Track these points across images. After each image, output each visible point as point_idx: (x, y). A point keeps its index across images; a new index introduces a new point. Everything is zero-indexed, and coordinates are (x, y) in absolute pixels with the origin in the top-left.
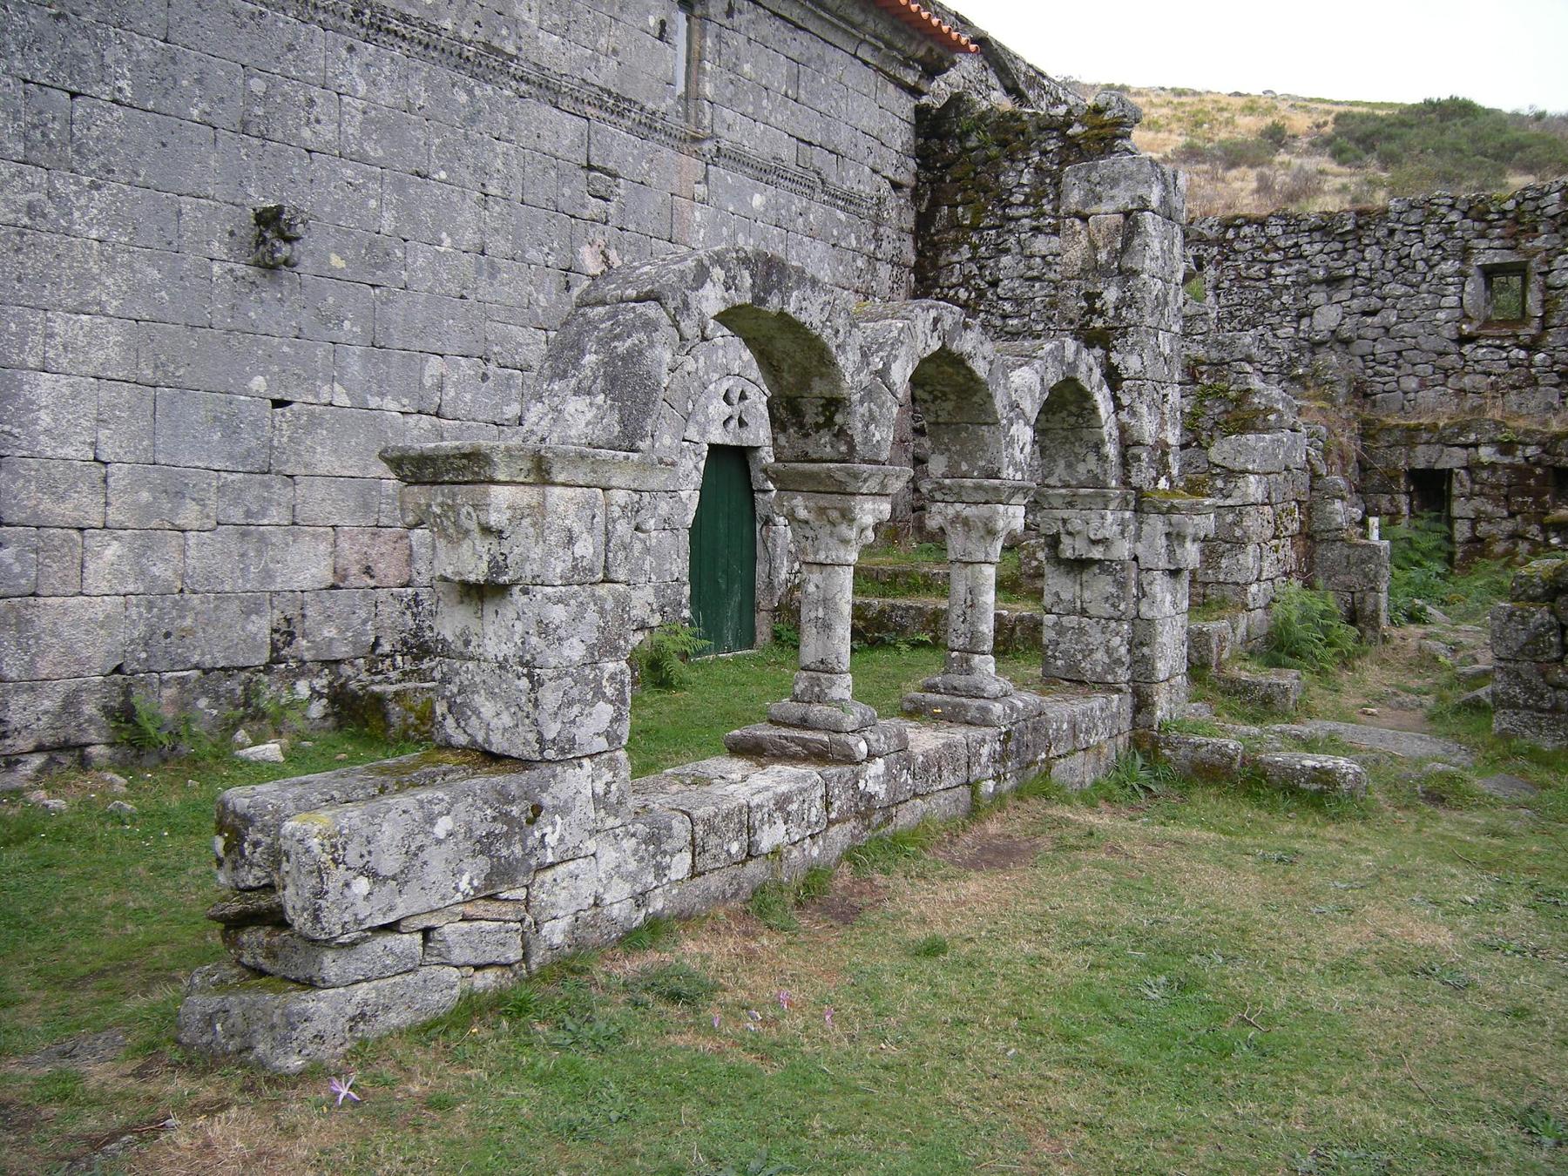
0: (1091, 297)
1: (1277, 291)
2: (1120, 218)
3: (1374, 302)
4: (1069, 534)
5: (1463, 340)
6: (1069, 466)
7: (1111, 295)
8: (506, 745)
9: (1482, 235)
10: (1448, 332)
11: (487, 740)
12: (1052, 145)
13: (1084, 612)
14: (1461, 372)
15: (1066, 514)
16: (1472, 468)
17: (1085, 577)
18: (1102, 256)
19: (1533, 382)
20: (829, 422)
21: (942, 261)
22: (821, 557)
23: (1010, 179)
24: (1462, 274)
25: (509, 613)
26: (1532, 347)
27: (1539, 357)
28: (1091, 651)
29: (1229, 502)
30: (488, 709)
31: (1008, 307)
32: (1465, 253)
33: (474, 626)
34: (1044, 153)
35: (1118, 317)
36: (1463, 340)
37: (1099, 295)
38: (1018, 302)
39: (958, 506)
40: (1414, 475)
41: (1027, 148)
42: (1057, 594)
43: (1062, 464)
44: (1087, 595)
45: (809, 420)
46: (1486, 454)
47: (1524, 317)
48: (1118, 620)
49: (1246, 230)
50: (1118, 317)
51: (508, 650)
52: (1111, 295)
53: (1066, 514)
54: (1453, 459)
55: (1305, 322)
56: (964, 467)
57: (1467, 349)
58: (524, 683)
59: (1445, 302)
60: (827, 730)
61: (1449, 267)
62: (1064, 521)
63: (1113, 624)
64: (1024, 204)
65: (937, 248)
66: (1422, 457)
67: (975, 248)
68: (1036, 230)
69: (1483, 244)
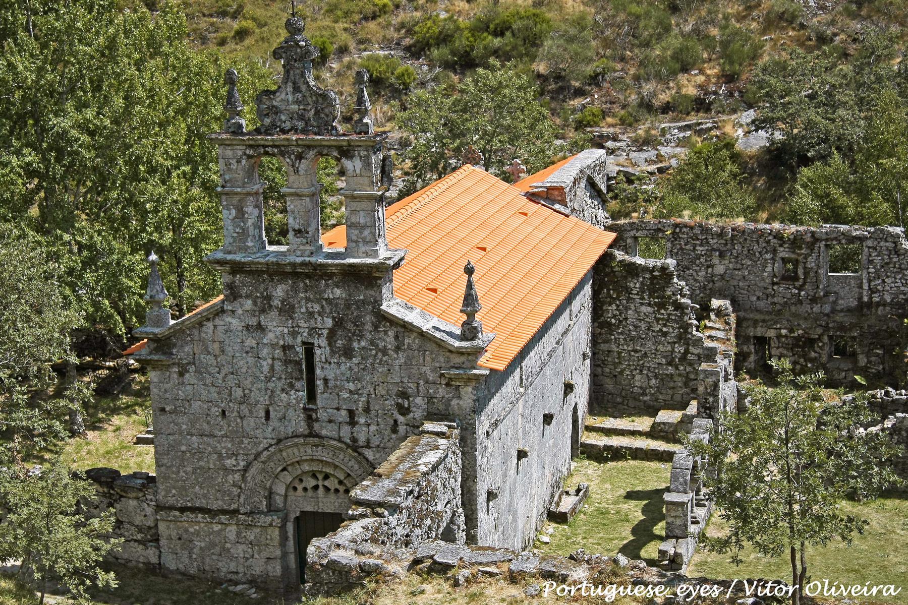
0: (706, 399)
1: (698, 257)
3: (739, 266)
5: (774, 284)
9: (781, 246)
10: (768, 281)
12: (647, 276)
14: (773, 296)
16: (779, 336)
19: (801, 302)
21: (605, 308)
23: (632, 285)
24: (773, 259)
26: (800, 289)
27: (803, 293)
31: (631, 328)
32: (774, 251)
34: (644, 278)
36: (774, 284)
38: (636, 327)
40: (755, 337)
41: (638, 276)
46: (784, 332)
47: (796, 278)
49: (685, 230)
54: (771, 333)
55: (710, 270)
57: (775, 287)
59: (767, 269)
61: (768, 256)
64: (637, 294)
65: (603, 303)
66: (759, 331)
67: (618, 306)
68: (642, 304)
69: (782, 249)
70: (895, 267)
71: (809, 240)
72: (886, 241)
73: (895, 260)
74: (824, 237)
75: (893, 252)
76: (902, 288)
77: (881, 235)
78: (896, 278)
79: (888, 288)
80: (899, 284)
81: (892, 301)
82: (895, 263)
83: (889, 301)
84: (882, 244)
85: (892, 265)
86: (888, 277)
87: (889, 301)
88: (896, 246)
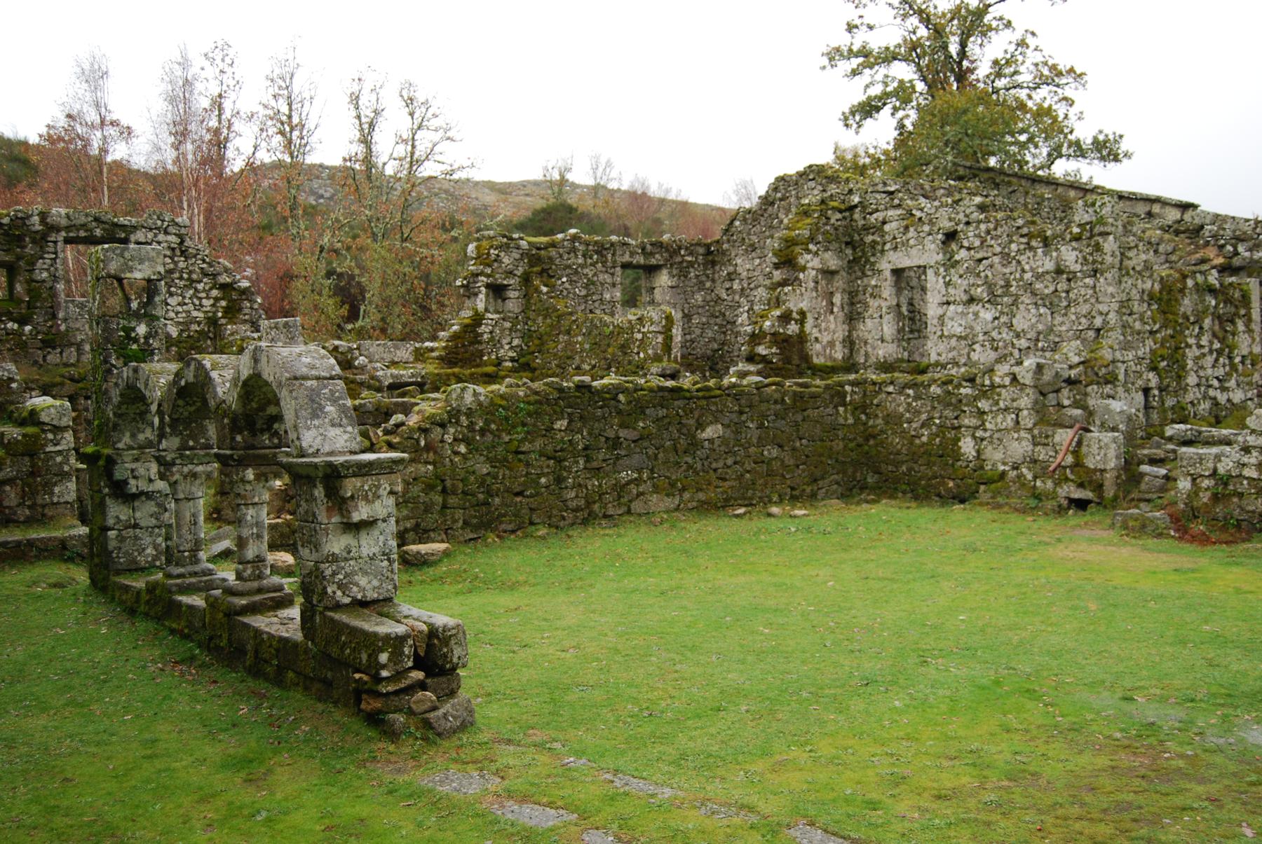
2: (144, 283)
4: (135, 477)
6: (133, 436)
7: (142, 329)
8: (376, 595)
11: (364, 596)
13: (136, 526)
15: (134, 466)
17: (136, 504)
18: (134, 305)
20: (269, 428)
22: (256, 500)
25: (376, 533)
27: (28, 328)
28: (144, 550)
29: (58, 448)
30: (363, 581)
33: (353, 543)
35: (147, 342)
37: (133, 329)
39: (190, 467)
42: (117, 517)
43: (128, 434)
44: (138, 515)
45: (258, 426)
48: (159, 527)
50: (147, 342)
51: (376, 550)
52: (142, 329)
53: (134, 466)
56: (191, 443)
58: (386, 563)
60: (275, 591)
62: (133, 471)
63: (157, 530)
70: (181, 278)
71: (38, 228)
72: (166, 233)
73: (182, 265)
74: (64, 222)
75: (178, 253)
76: (195, 314)
77: (159, 223)
78: (184, 297)
79: (172, 315)
80: (191, 307)
81: (180, 335)
82: (181, 272)
83: (175, 335)
84: (161, 237)
85: (177, 275)
86: (171, 295)
87: (175, 335)
88: (182, 242)
